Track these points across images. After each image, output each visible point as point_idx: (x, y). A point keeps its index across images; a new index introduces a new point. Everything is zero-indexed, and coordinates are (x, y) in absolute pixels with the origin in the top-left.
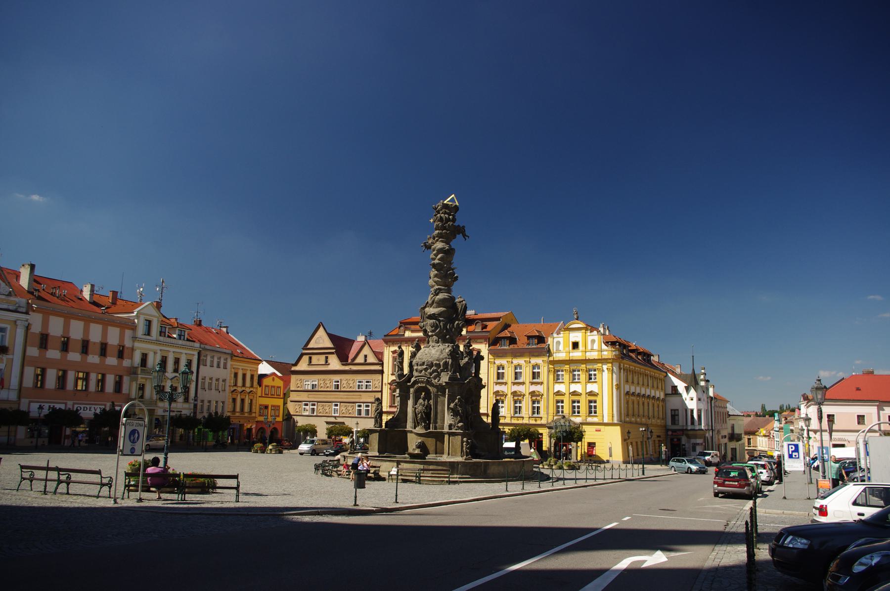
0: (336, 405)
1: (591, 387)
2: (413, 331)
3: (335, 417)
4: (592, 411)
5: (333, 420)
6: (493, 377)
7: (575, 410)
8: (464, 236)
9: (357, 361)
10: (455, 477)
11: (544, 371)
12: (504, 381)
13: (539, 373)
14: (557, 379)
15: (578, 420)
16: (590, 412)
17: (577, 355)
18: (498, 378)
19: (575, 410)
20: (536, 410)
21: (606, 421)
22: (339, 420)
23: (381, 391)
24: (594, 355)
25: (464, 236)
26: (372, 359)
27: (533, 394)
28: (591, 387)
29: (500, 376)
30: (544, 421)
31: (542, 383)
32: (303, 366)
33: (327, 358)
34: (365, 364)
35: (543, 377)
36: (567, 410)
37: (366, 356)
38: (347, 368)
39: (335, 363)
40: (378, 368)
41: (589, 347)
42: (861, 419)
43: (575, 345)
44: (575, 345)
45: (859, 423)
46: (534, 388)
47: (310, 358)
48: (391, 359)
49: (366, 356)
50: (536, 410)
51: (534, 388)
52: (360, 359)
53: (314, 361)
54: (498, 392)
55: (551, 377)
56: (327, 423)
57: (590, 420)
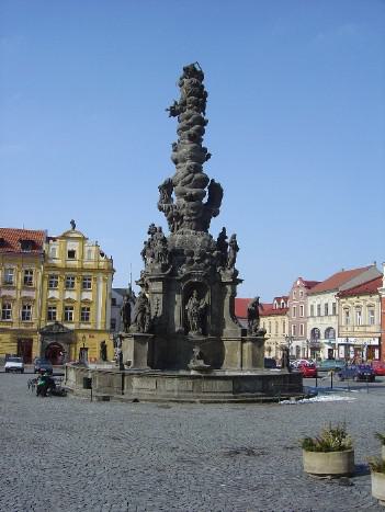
1: (87, 295)
4: (85, 317)
7: (67, 317)
10: (351, 382)
14: (52, 285)
15: (71, 327)
16: (83, 319)
17: (74, 263)
19: (67, 317)
20: (25, 316)
21: (99, 328)
24: (91, 265)
27: (25, 299)
28: (87, 295)
30: (35, 327)
31: (34, 289)
36: (59, 318)
41: (86, 257)
43: (71, 254)
44: (71, 254)
46: (25, 293)
50: (25, 316)
51: (25, 293)
55: (46, 283)
57: (83, 326)
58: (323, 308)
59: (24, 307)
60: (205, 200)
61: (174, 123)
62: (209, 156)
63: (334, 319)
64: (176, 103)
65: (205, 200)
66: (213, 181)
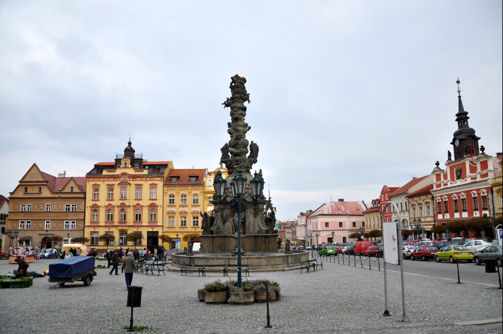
0: (48, 222)
2: (108, 171)
3: (47, 231)
5: (45, 233)
6: (167, 202)
8: (249, 101)
9: (65, 191)
11: (200, 198)
12: (174, 204)
13: (173, 200)
18: (170, 203)
22: (48, 233)
23: (85, 212)
25: (249, 101)
26: (76, 190)
29: (172, 201)
31: (199, 206)
32: (20, 194)
33: (40, 188)
34: (72, 192)
35: (200, 202)
37: (72, 188)
38: (57, 196)
39: (46, 193)
40: (83, 196)
42: (341, 224)
45: (340, 226)
47: (26, 189)
48: (92, 190)
49: (72, 188)
52: (68, 189)
53: (29, 190)
54: (170, 211)
56: (39, 234)
58: (400, 205)
59: (194, 218)
60: (248, 155)
61: (229, 109)
62: (250, 128)
63: (407, 214)
64: (228, 99)
65: (248, 155)
66: (252, 142)
